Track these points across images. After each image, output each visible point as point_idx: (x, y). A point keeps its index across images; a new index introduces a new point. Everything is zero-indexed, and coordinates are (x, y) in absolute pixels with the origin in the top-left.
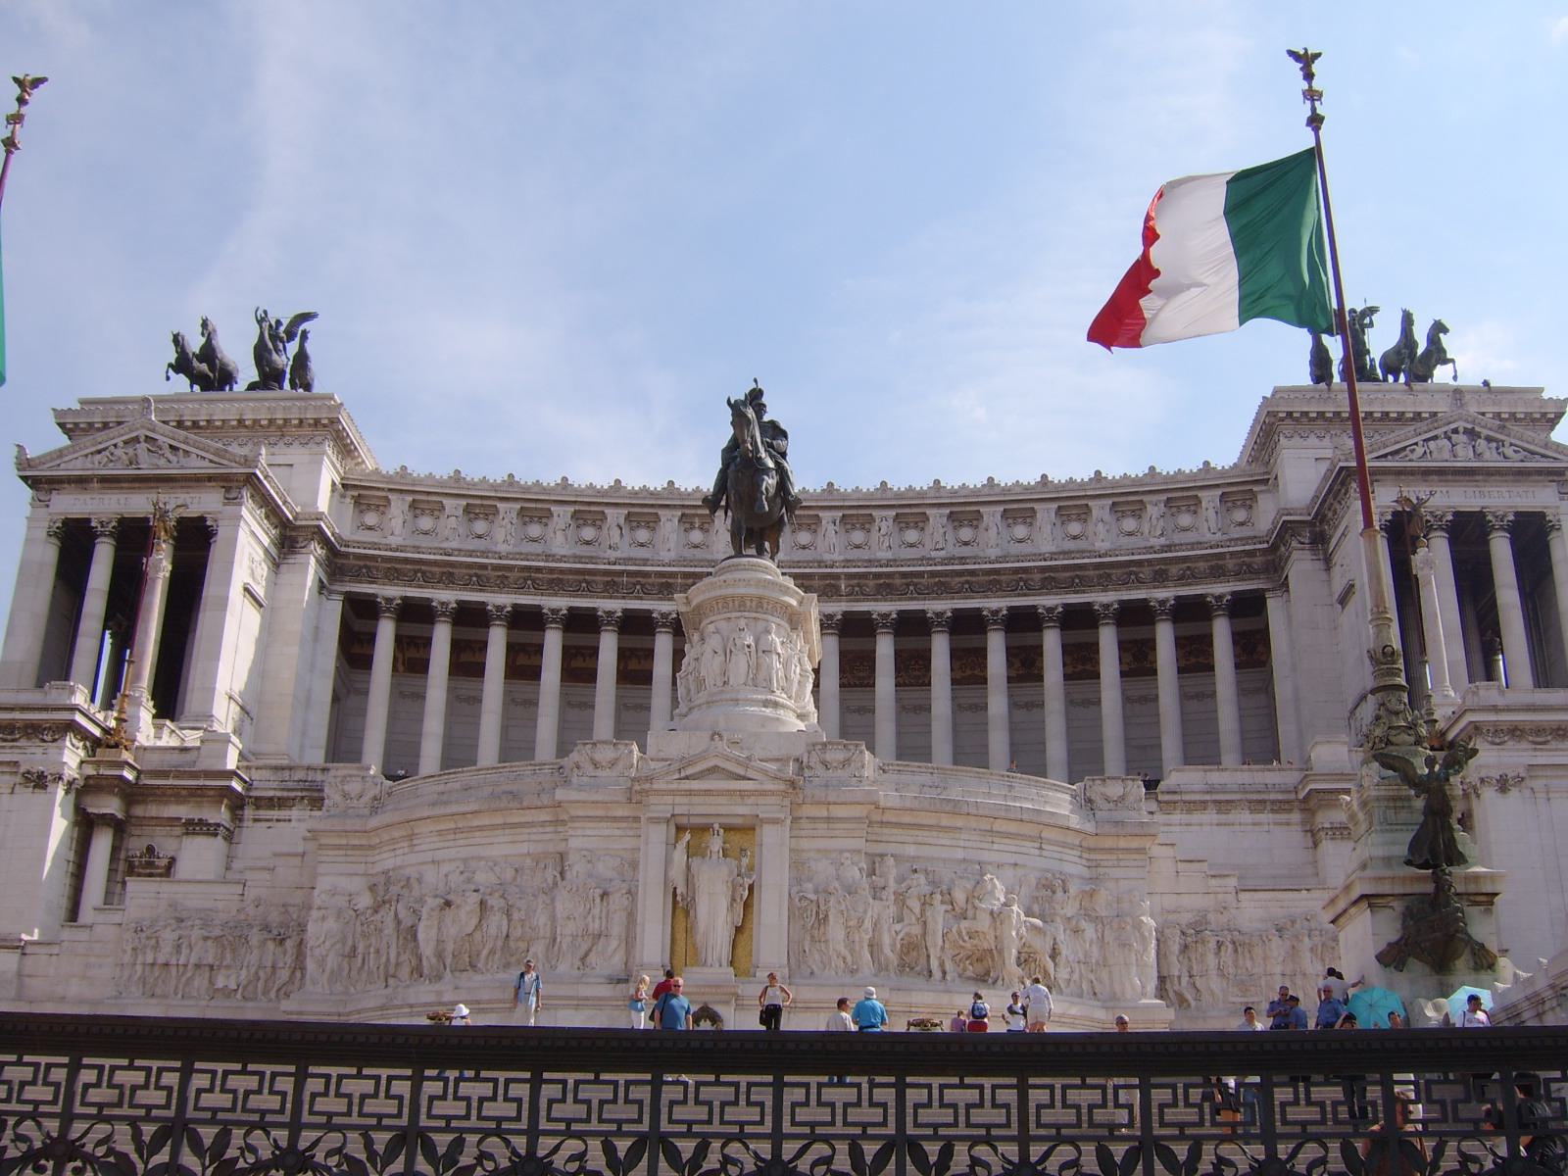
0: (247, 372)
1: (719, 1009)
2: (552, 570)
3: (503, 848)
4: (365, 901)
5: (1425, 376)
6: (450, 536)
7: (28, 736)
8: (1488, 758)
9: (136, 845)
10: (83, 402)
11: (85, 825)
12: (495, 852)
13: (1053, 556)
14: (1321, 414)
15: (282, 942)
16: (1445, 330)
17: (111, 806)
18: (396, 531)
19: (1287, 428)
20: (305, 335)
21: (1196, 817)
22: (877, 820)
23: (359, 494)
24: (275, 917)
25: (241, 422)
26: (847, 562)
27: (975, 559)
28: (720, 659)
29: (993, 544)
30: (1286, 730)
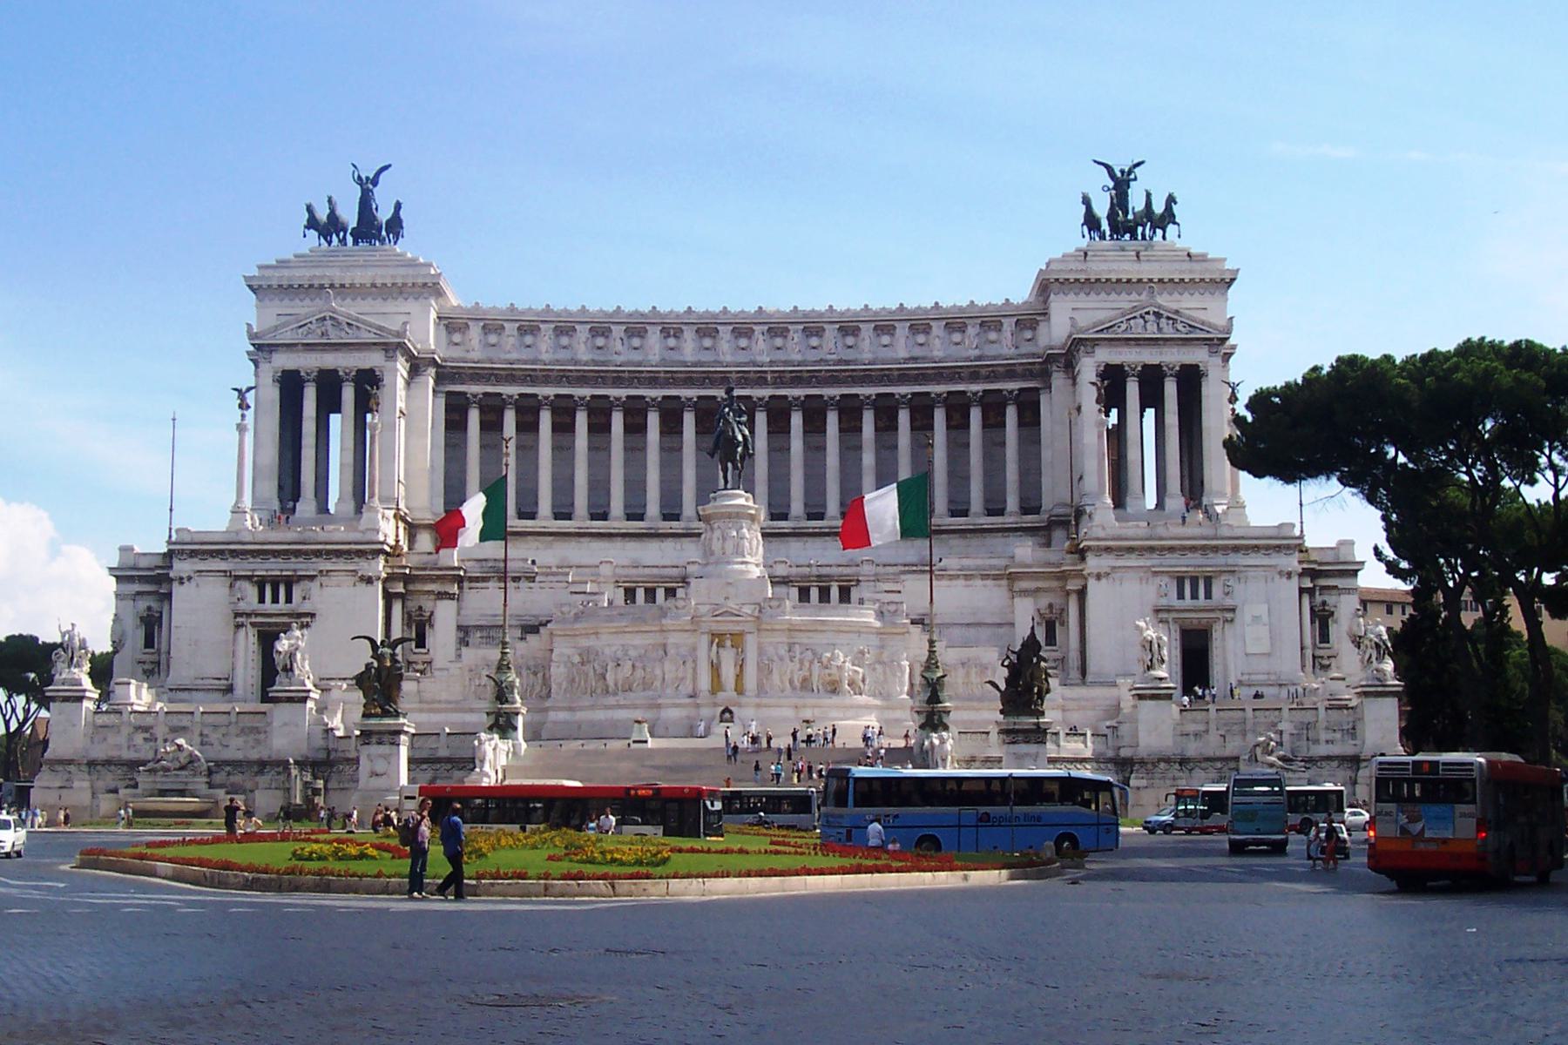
0: (352, 223)
3: (638, 640)
4: (577, 659)
6: (510, 350)
8: (1093, 563)
9: (412, 605)
10: (260, 267)
11: (389, 598)
13: (907, 360)
14: (1077, 280)
15: (535, 674)
17: (400, 589)
18: (474, 349)
20: (398, 206)
21: (955, 582)
22: (792, 629)
23: (451, 324)
24: (531, 663)
25: (374, 285)
26: (772, 363)
27: (855, 362)
29: (868, 350)
30: (1046, 482)
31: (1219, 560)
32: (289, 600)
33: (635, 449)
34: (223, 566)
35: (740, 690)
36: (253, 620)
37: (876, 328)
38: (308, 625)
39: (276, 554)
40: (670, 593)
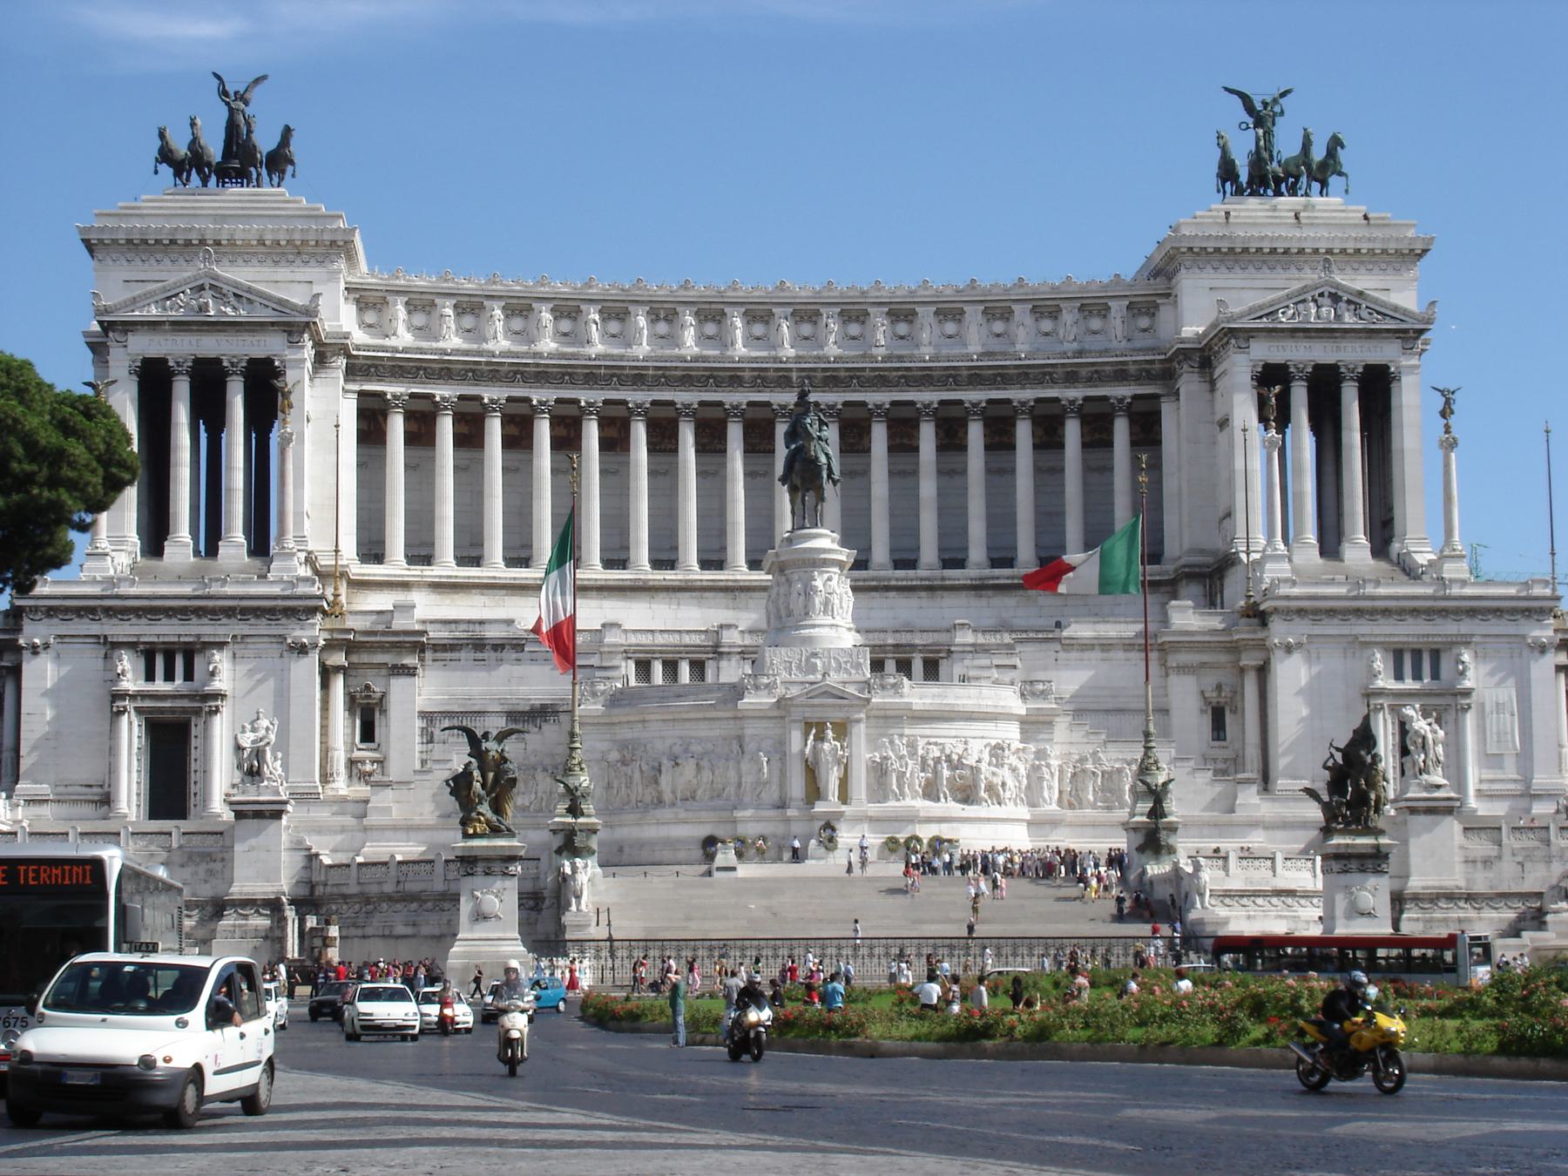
1: (833, 823)
2: (538, 365)
4: (614, 756)
5: (1324, 184)
7: (288, 617)
8: (1279, 632)
11: (326, 673)
12: (702, 734)
14: (1218, 250)
16: (1343, 147)
17: (339, 659)
19: (1189, 256)
20: (287, 132)
21: (1087, 655)
24: (547, 761)
25: (261, 242)
26: (798, 359)
27: (911, 358)
28: (802, 598)
31: (1450, 628)
32: (189, 676)
33: (951, 473)
34: (95, 628)
35: (844, 798)
36: (139, 704)
37: (937, 313)
38: (217, 711)
39: (169, 612)
40: (698, 667)
